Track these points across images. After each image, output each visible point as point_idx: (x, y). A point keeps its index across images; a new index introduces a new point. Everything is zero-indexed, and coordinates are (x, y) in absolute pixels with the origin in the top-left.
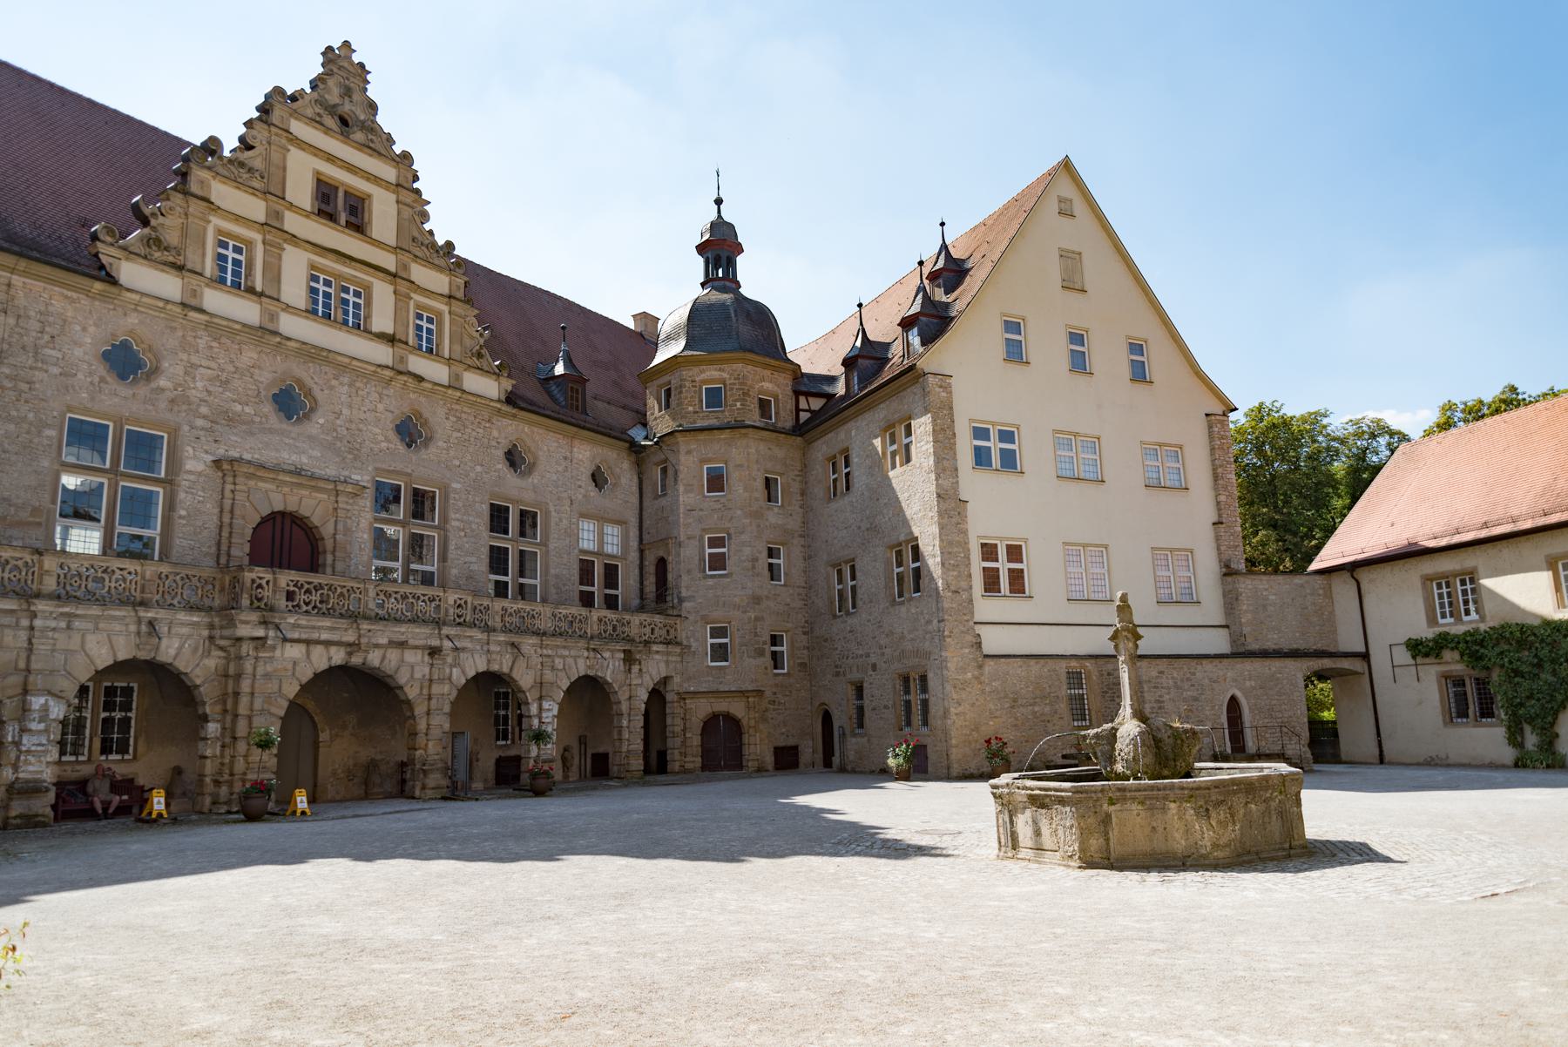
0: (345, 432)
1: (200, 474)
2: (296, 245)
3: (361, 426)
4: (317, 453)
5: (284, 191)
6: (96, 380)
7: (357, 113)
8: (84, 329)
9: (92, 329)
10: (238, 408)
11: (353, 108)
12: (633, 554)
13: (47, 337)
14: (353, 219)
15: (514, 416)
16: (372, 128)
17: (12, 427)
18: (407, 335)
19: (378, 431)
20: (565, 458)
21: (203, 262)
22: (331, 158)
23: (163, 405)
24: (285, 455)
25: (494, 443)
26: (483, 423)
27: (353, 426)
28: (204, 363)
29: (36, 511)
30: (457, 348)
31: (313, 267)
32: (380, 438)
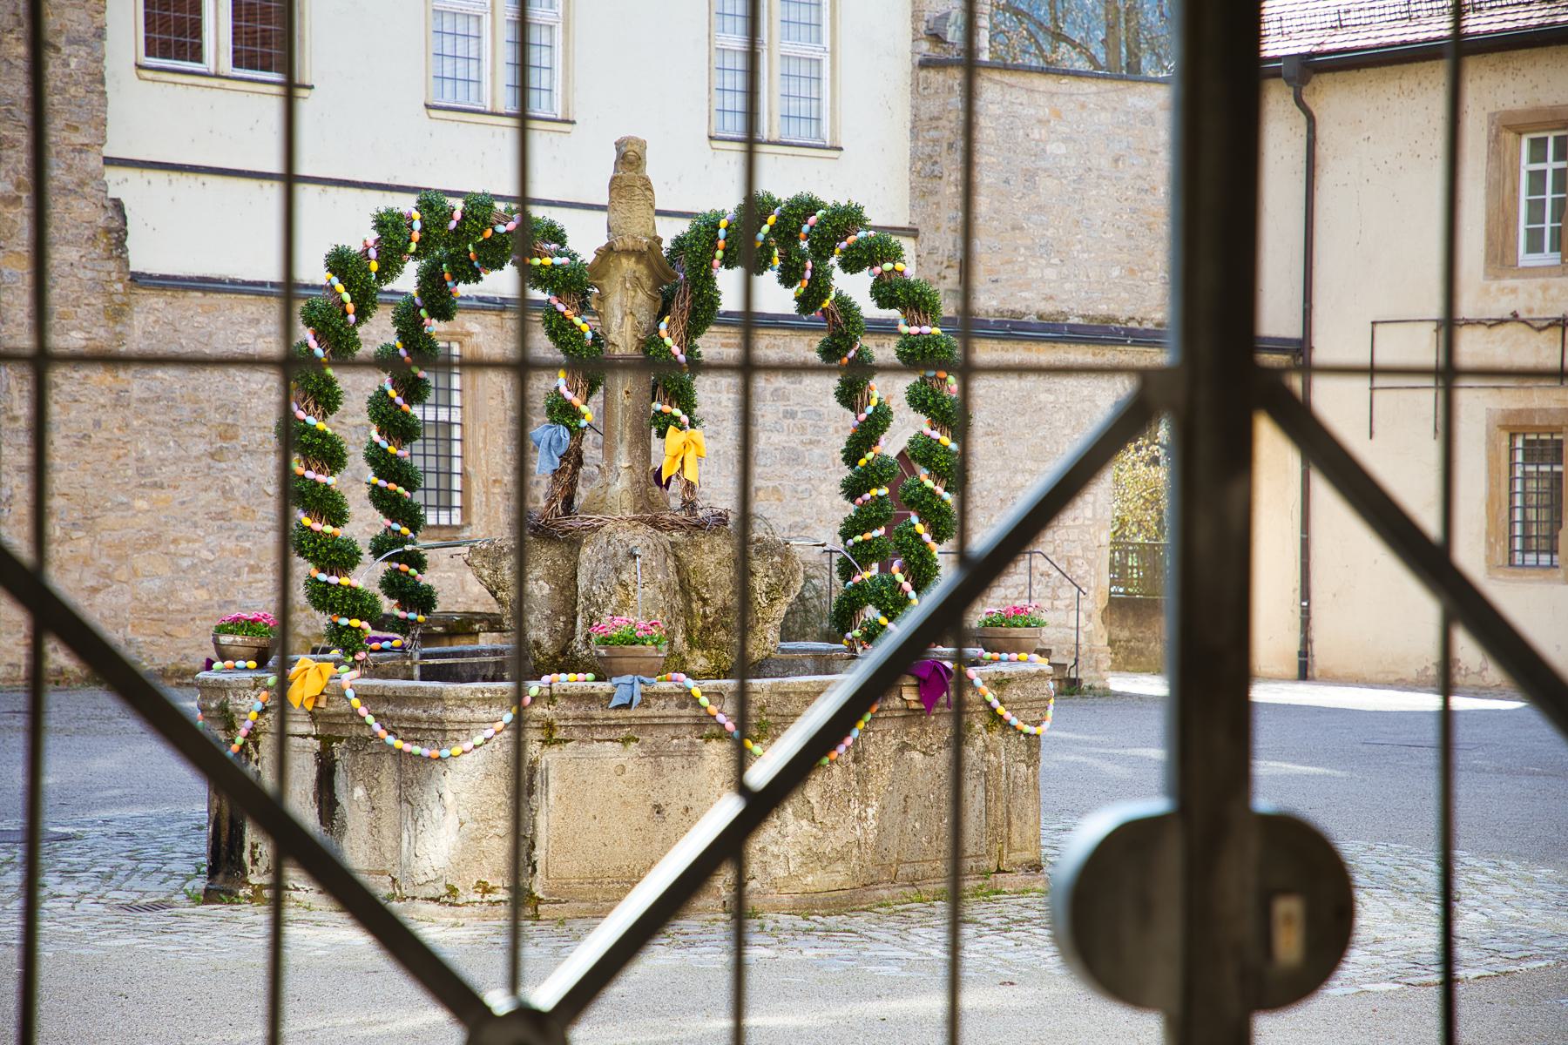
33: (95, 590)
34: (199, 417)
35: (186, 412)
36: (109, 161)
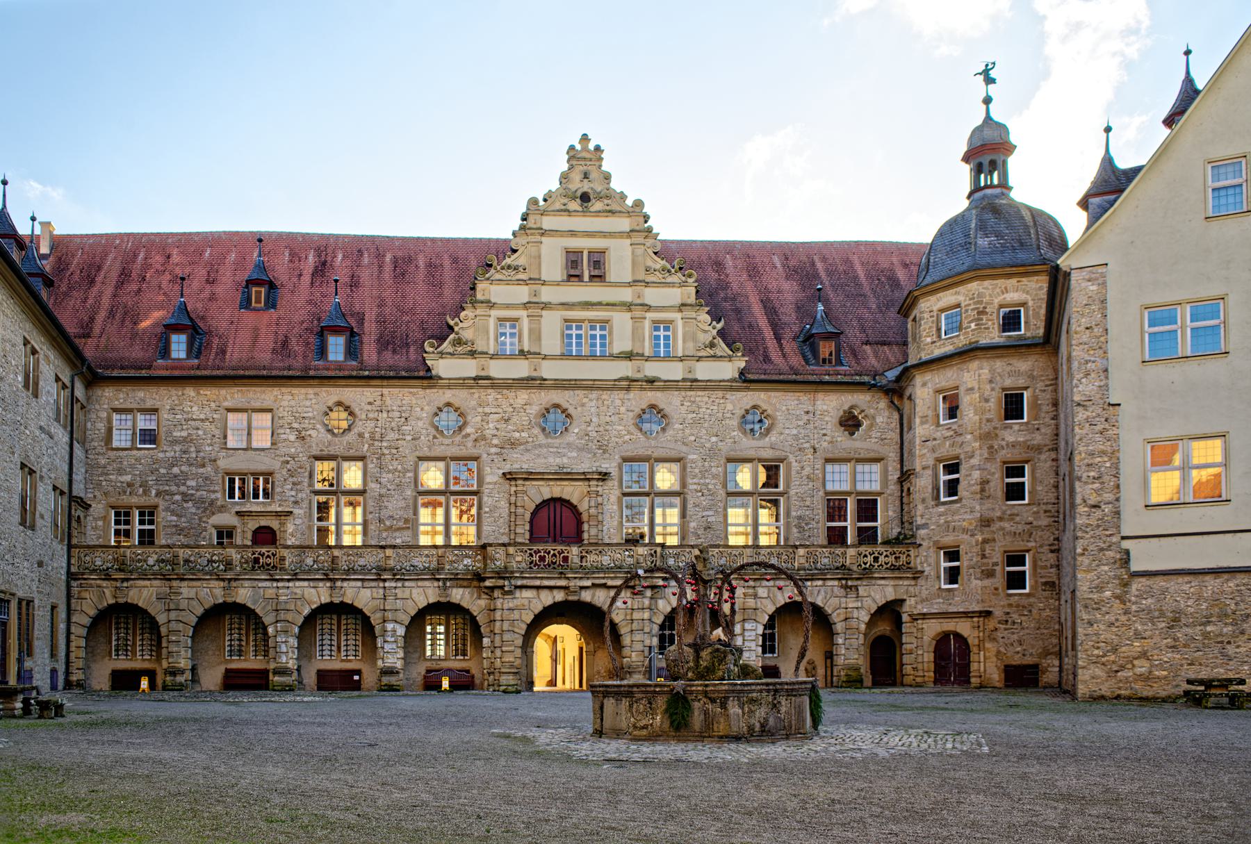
0: (595, 434)
1: (495, 483)
2: (551, 309)
3: (607, 427)
4: (574, 454)
5: (540, 273)
6: (431, 437)
7: (595, 188)
8: (422, 409)
9: (426, 408)
10: (517, 435)
11: (592, 185)
12: (892, 487)
13: (403, 420)
14: (596, 273)
15: (748, 389)
16: (609, 195)
17: (390, 475)
18: (643, 348)
19: (621, 428)
20: (807, 412)
21: (488, 344)
22: (572, 233)
23: (470, 444)
24: (551, 460)
25: (729, 415)
26: (717, 401)
27: (601, 429)
28: (493, 410)
29: (406, 521)
30: (690, 345)
31: (566, 321)
32: (624, 432)
33: (1117, 671)
34: (1162, 614)
35: (1156, 614)
36: (1123, 538)
